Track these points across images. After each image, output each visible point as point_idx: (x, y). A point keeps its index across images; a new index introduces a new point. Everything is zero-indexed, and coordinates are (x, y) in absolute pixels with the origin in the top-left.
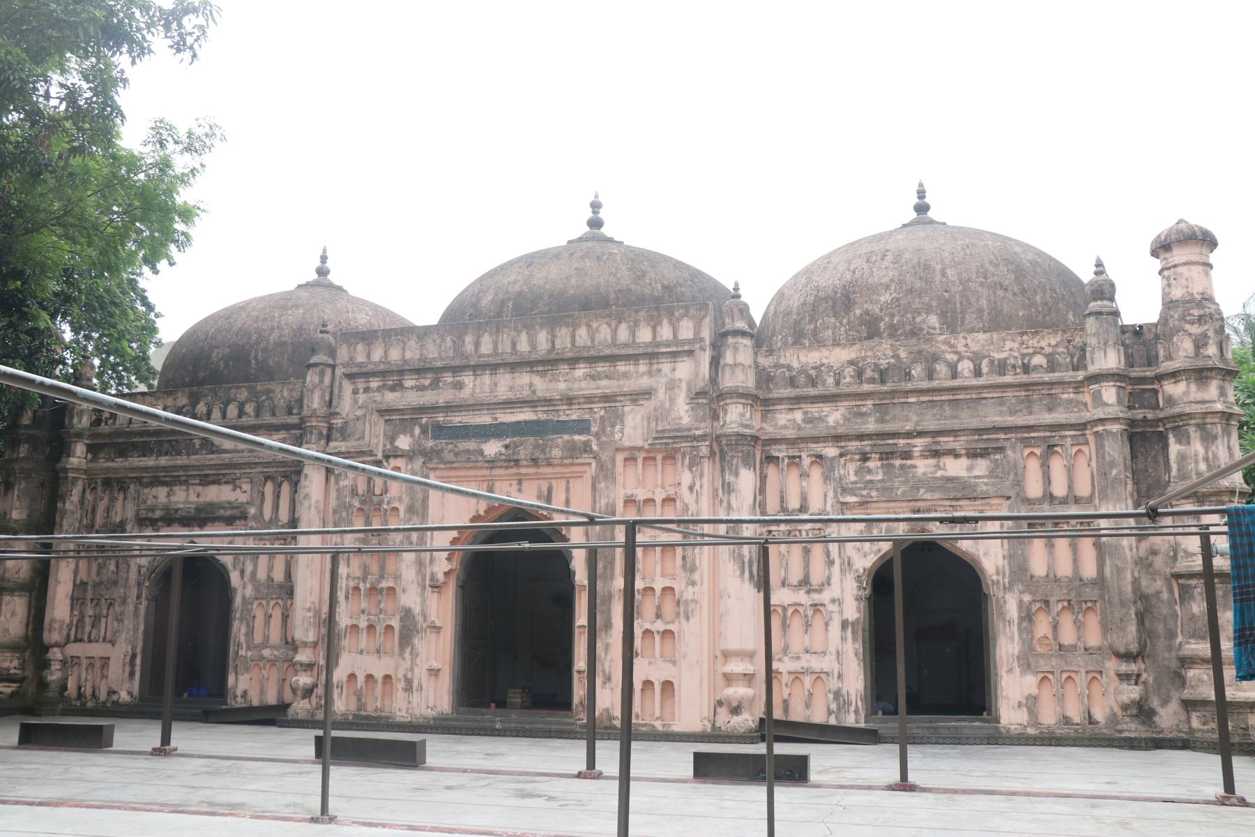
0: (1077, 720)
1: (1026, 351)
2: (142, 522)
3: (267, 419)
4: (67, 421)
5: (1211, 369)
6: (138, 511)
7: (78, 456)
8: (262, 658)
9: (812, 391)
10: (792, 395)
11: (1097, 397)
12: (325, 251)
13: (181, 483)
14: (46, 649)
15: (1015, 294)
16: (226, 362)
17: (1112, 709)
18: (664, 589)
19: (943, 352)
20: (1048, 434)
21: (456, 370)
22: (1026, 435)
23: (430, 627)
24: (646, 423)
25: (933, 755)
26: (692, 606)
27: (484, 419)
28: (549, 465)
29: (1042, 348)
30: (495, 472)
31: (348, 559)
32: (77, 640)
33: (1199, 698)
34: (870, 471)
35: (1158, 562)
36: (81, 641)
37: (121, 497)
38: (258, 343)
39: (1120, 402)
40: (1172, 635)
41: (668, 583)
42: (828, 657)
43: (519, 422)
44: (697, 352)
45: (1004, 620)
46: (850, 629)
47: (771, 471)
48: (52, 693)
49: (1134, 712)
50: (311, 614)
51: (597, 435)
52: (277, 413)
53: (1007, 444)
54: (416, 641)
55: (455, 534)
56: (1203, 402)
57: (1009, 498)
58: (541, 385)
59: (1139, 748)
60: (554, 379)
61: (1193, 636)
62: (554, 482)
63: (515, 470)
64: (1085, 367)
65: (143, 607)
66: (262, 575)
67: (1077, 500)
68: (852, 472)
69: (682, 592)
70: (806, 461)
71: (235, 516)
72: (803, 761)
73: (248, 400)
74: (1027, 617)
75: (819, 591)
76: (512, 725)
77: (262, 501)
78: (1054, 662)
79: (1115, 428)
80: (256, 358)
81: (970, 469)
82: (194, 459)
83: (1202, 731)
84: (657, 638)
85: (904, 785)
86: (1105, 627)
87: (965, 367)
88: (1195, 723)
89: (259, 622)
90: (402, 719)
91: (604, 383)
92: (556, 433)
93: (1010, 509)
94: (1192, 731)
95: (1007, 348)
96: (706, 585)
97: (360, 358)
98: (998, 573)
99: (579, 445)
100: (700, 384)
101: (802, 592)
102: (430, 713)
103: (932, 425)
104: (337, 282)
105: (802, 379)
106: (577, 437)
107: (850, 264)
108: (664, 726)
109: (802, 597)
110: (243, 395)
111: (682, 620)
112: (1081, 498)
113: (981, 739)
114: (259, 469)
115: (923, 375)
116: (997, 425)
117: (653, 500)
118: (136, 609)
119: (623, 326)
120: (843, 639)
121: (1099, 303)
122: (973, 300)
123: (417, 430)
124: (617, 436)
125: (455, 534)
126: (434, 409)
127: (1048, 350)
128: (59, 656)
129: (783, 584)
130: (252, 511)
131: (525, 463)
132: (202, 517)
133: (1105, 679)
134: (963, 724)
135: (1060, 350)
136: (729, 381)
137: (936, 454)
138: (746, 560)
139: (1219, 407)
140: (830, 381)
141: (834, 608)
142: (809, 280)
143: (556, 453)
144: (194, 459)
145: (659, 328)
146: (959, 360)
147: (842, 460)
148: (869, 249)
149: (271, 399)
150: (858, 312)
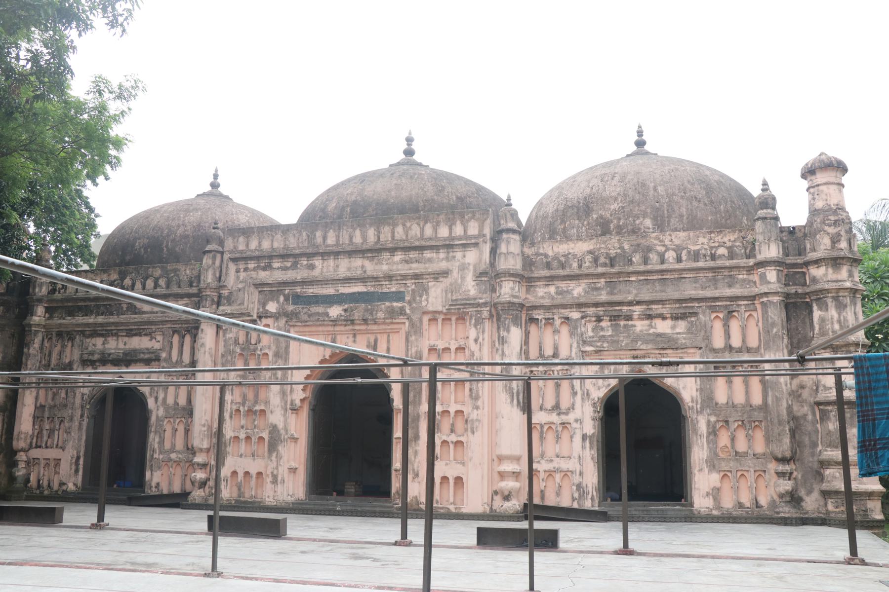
0: (748, 504)
1: (713, 245)
2: (85, 363)
3: (175, 289)
4: (31, 290)
5: (843, 258)
6: (82, 355)
7: (39, 316)
8: (170, 460)
9: (562, 272)
10: (548, 275)
11: (763, 277)
12: (216, 171)
13: (113, 335)
14: (15, 453)
15: (705, 205)
16: (146, 249)
17: (772, 497)
18: (457, 412)
19: (655, 245)
20: (728, 303)
21: (310, 256)
25: (647, 530)
26: (476, 424)
27: (330, 291)
28: (375, 323)
30: (337, 328)
31: (232, 389)
32: (37, 447)
33: (833, 489)
34: (602, 329)
35: (805, 394)
36: (40, 447)
37: (70, 344)
38: (168, 236)
39: (779, 281)
40: (814, 445)
41: (459, 408)
42: (573, 459)
43: (354, 293)
44: (481, 245)
45: (697, 434)
46: (588, 441)
47: (533, 329)
48: (19, 485)
49: (788, 499)
50: (205, 429)
51: (409, 303)
52: (182, 285)
53: (700, 310)
54: (280, 448)
55: (308, 372)
56: (837, 281)
57: (700, 348)
58: (370, 267)
59: (791, 525)
60: (380, 262)
61: (829, 446)
62: (379, 336)
63: (351, 327)
64: (755, 256)
65: (85, 423)
66: (170, 401)
67: (748, 350)
68: (590, 330)
69: (469, 414)
70: (558, 322)
71: (152, 358)
72: (555, 533)
73: (161, 277)
74: (713, 432)
75: (567, 414)
77: (171, 348)
78: (732, 464)
79: (776, 299)
80: (167, 245)
81: (673, 327)
82: (123, 318)
83: (835, 512)
84: (452, 446)
85: (626, 551)
86: (768, 440)
87: (671, 255)
88: (830, 507)
89: (168, 434)
90: (269, 504)
91: (414, 265)
93: (701, 356)
94: (828, 512)
95: (700, 242)
96: (486, 409)
97: (241, 247)
98: (692, 401)
99: (397, 309)
100: (482, 267)
101: (554, 414)
102: (290, 499)
103: (647, 297)
104: (225, 193)
105: (555, 264)
106: (395, 304)
107: (589, 182)
108: (456, 508)
109: (554, 418)
110: (158, 272)
111: (469, 433)
112: (751, 349)
113: (680, 518)
114: (169, 326)
115: (640, 261)
116: (692, 296)
117: (449, 349)
118: (80, 424)
119: (428, 225)
120: (583, 448)
121: (765, 211)
122: (676, 208)
123: (282, 299)
124: (424, 304)
125: (308, 372)
126: (293, 283)
127: (729, 244)
128: (24, 458)
129: (541, 409)
130: (164, 355)
131: (358, 322)
132: (128, 359)
133: (767, 476)
134: (667, 507)
135: (737, 244)
136: (503, 265)
137: (649, 317)
138: (515, 391)
139: (848, 284)
140: (575, 265)
141: (577, 425)
142: (560, 194)
143: (381, 315)
144: (123, 318)
145: (453, 227)
146: (666, 251)
147: (583, 321)
148: (603, 172)
149: (178, 276)
150: (595, 216)
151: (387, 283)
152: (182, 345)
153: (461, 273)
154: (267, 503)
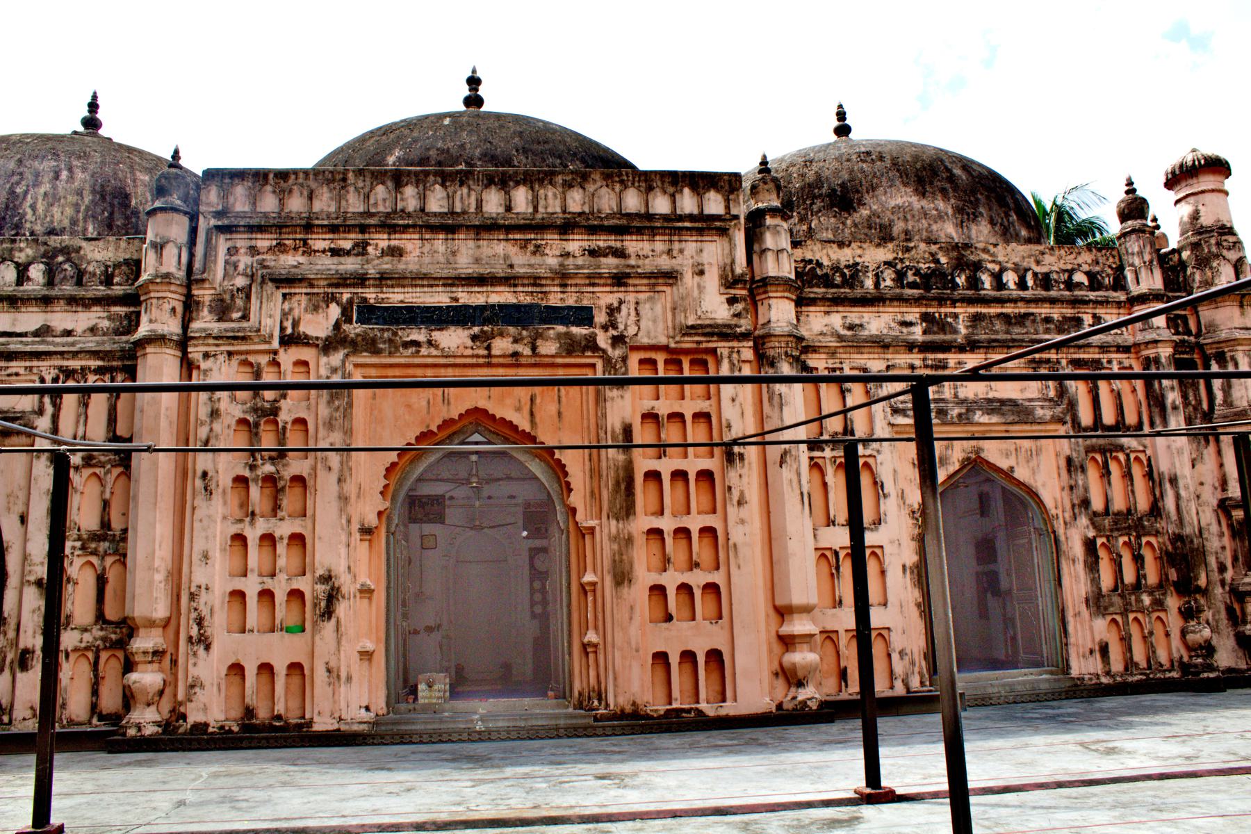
3: (68, 289)
12: (95, 97)
20: (1097, 356)
22: (1076, 356)
23: (361, 591)
26: (743, 551)
27: (439, 298)
29: (1079, 265)
51: (605, 328)
55: (393, 456)
76: (500, 724)
87: (1010, 278)
105: (838, 279)
106: (575, 330)
124: (632, 330)
126: (361, 280)
127: (1086, 268)
131: (501, 360)
140: (869, 283)
143: (548, 348)
145: (678, 196)
146: (1003, 270)
151: (558, 289)
153: (697, 278)
154: (317, 727)
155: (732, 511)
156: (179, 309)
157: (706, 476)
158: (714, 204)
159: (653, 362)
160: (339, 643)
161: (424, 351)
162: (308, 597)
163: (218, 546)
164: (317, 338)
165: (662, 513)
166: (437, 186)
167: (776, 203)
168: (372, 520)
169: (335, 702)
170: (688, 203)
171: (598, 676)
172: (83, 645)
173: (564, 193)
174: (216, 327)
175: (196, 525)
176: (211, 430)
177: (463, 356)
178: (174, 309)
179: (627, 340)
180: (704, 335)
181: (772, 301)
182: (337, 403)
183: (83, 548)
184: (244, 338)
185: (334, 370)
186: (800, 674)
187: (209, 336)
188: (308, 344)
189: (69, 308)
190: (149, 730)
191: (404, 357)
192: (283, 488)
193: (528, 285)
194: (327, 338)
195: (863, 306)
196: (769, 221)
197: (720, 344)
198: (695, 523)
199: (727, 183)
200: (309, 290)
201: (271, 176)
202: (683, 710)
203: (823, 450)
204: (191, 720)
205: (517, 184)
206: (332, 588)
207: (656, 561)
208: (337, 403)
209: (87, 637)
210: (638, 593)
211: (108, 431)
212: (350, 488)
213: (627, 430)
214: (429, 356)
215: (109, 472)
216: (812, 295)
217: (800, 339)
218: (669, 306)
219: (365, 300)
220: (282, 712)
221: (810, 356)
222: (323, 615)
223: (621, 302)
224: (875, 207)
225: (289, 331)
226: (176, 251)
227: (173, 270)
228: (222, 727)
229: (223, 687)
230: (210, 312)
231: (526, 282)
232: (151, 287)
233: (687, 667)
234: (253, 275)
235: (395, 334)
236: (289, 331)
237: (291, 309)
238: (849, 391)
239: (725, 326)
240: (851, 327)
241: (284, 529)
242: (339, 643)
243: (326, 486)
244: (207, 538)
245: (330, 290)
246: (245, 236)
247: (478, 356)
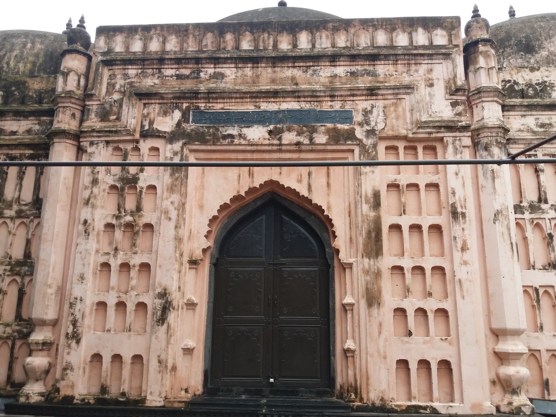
3: (15, 106)
18: (434, 268)
23: (187, 304)
24: (408, 115)
26: (466, 285)
28: (312, 151)
41: (439, 262)
51: (361, 124)
90: (154, 404)
92: (318, 121)
105: (531, 92)
106: (339, 126)
126: (195, 95)
131: (289, 148)
143: (321, 138)
145: (414, 34)
151: (328, 99)
152: (21, 177)
155: (457, 255)
156: (78, 114)
157: (436, 228)
158: (440, 38)
159: (396, 148)
160: (168, 342)
161: (236, 141)
162: (150, 307)
163: (91, 271)
164: (165, 132)
165: (403, 255)
166: (247, 33)
167: (486, 36)
168: (198, 254)
169: (162, 385)
170: (421, 38)
171: (355, 375)
172: (5, 335)
173: (333, 34)
174: (99, 125)
175: (78, 255)
176: (92, 192)
177: (262, 145)
178: (73, 115)
179: (377, 133)
180: (434, 127)
181: (485, 104)
182: (177, 175)
183: (11, 270)
184: (116, 132)
185: (176, 154)
186: (515, 385)
187: (93, 131)
188: (159, 137)
189: (15, 118)
190: (35, 399)
191: (223, 145)
192: (138, 231)
193: (308, 97)
194: (172, 132)
195: (551, 110)
196: (481, 48)
197: (446, 134)
198: (428, 264)
199: (449, 24)
200: (161, 101)
201: (140, 29)
202: (420, 407)
203: (523, 213)
204: (63, 393)
205: (301, 30)
206: (166, 302)
207: (399, 289)
208: (177, 175)
209: (9, 330)
210: (386, 313)
211: (33, 195)
212: (184, 232)
213: (377, 195)
214: (240, 145)
215: (32, 221)
216: (512, 104)
217: (506, 131)
218: (407, 109)
219: (198, 107)
220: (126, 390)
221: (511, 146)
222: (158, 321)
223: (373, 107)
224: (552, 49)
225: (147, 128)
226: (76, 78)
227: (74, 89)
228: (83, 400)
229: (87, 370)
230: (96, 116)
231: (306, 94)
232: (59, 100)
233: (424, 372)
234: (125, 91)
235: (217, 130)
236: (147, 128)
237: (148, 114)
238: (542, 171)
239: (450, 121)
240: (542, 126)
241: (136, 260)
242: (168, 342)
243: (166, 230)
244: (84, 265)
245: (175, 101)
246: (121, 67)
247: (272, 145)
